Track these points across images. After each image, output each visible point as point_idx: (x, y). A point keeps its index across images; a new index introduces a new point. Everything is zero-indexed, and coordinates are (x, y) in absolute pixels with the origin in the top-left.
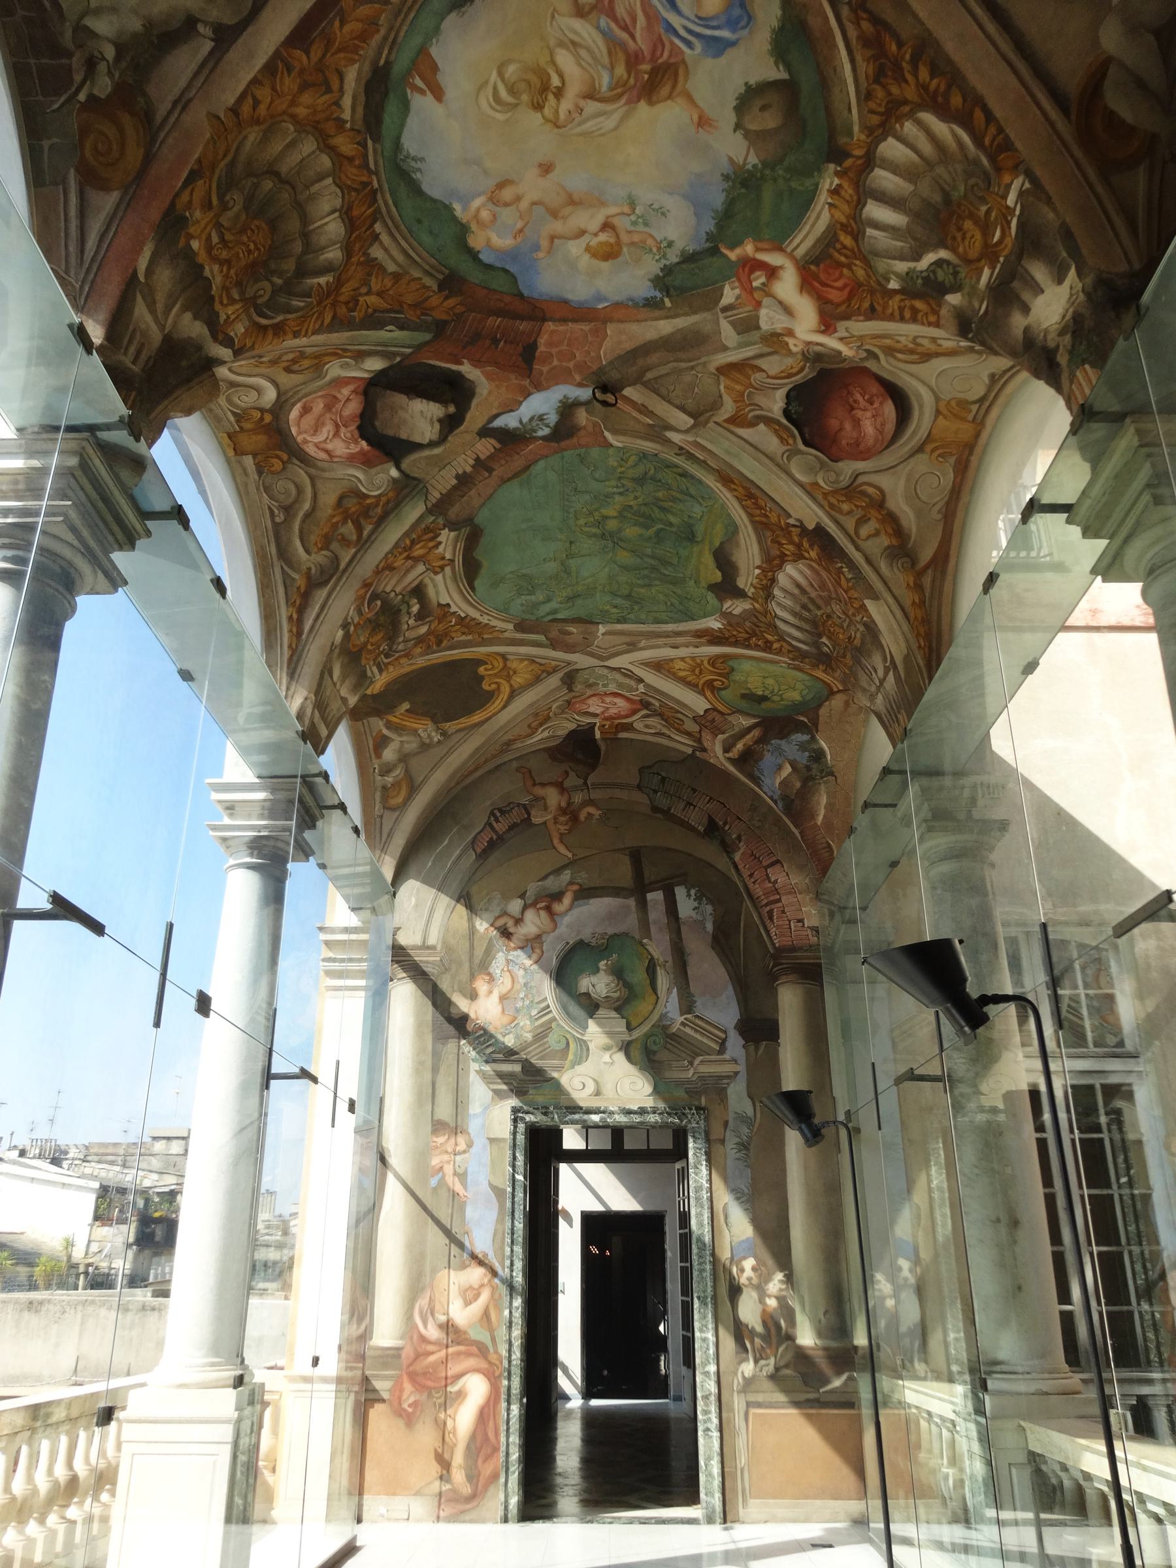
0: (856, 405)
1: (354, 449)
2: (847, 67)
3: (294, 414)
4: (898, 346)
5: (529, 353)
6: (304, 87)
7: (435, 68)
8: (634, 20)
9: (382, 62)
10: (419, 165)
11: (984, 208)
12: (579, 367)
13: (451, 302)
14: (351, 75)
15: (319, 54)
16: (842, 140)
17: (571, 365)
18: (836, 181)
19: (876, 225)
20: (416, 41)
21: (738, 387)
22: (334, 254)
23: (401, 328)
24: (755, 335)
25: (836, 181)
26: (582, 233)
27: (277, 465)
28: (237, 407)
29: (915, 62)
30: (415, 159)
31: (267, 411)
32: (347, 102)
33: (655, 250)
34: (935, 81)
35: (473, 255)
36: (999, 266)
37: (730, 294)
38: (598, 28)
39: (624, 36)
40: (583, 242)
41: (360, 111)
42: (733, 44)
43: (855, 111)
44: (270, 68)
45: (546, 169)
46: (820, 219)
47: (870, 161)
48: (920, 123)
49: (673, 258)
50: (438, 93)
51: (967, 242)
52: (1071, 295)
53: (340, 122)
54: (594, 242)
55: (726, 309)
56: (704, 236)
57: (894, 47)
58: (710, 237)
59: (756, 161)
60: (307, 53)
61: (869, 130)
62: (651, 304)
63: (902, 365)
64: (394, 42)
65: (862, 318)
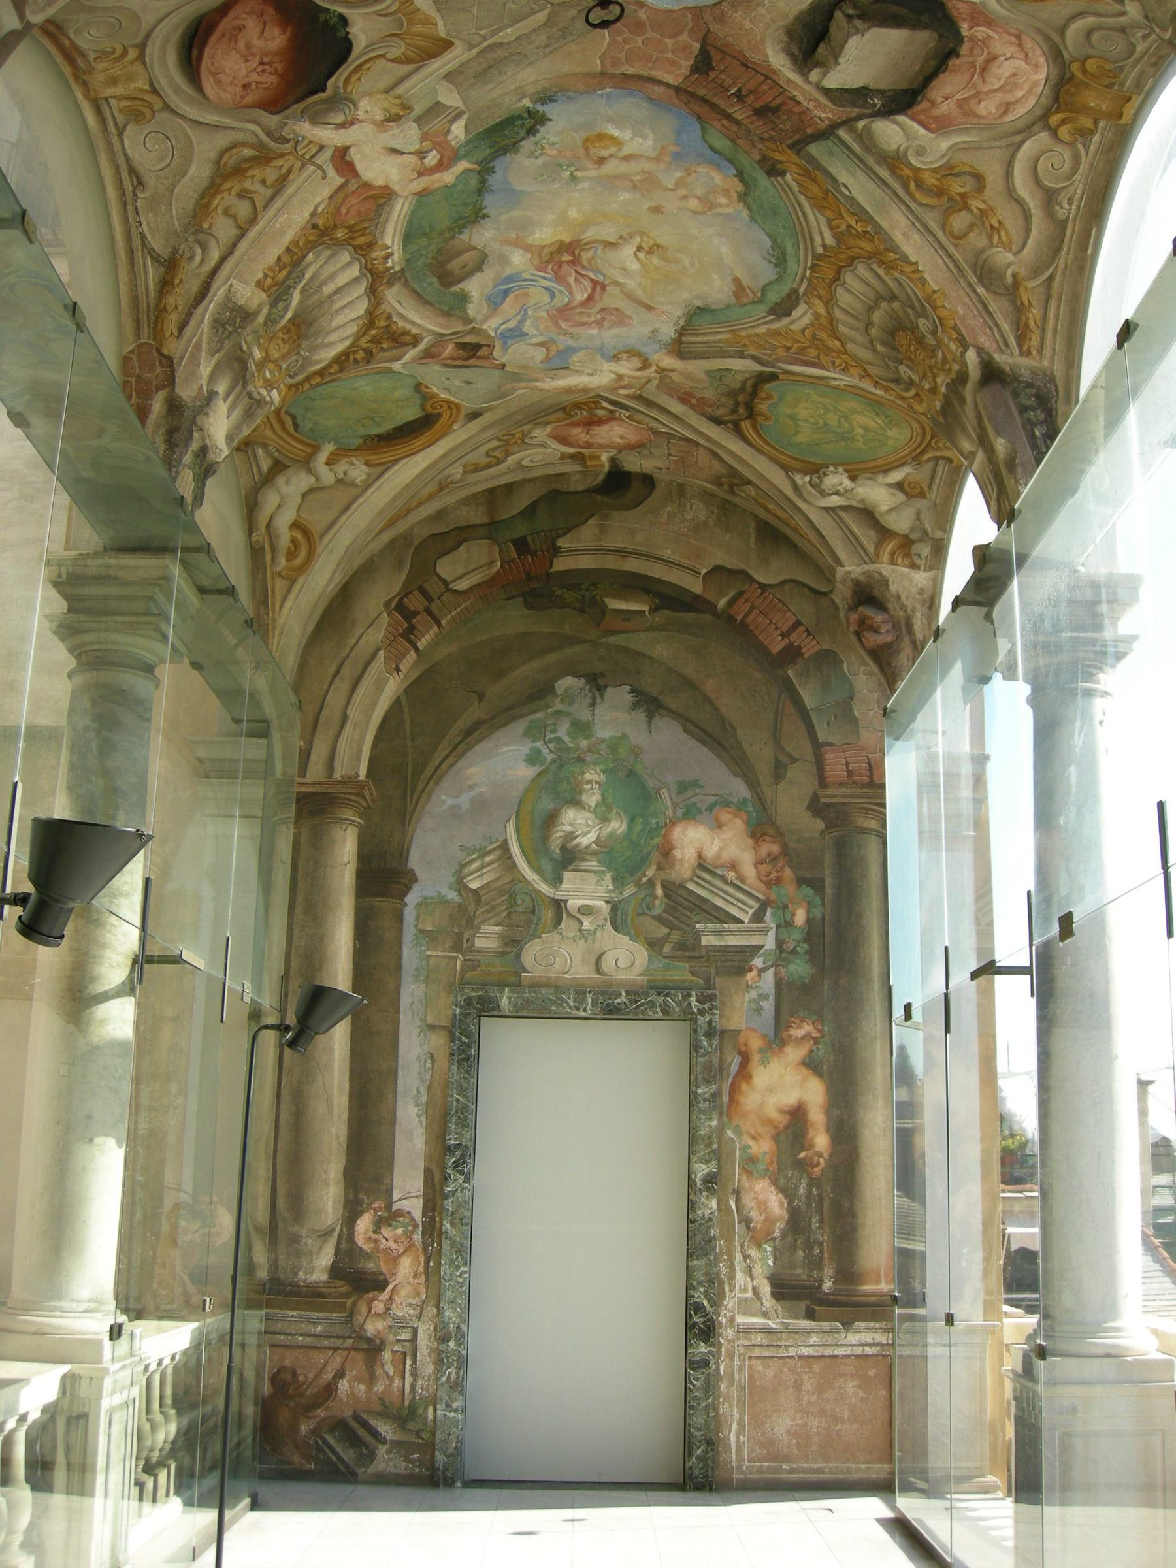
0: (260, 68)
1: (981, 32)
3: (1021, 111)
4: (257, 172)
5: (703, 64)
6: (831, 350)
8: (576, 279)
10: (768, 257)
12: (639, 27)
13: (777, 156)
17: (650, 33)
18: (390, 264)
19: (344, 267)
21: (418, 29)
22: (861, 269)
23: (835, 180)
24: (418, 109)
25: (390, 264)
26: (627, 158)
27: (1091, 65)
28: (1076, 159)
30: (770, 261)
31: (1050, 128)
33: (547, 147)
35: (740, 175)
37: (458, 131)
40: (626, 151)
45: (657, 210)
46: (391, 237)
49: (527, 145)
50: (736, 281)
51: (280, 342)
54: (613, 150)
55: (458, 116)
56: (496, 169)
57: (384, 346)
58: (491, 171)
59: (461, 237)
62: (546, 98)
63: (240, 136)
65: (320, 210)
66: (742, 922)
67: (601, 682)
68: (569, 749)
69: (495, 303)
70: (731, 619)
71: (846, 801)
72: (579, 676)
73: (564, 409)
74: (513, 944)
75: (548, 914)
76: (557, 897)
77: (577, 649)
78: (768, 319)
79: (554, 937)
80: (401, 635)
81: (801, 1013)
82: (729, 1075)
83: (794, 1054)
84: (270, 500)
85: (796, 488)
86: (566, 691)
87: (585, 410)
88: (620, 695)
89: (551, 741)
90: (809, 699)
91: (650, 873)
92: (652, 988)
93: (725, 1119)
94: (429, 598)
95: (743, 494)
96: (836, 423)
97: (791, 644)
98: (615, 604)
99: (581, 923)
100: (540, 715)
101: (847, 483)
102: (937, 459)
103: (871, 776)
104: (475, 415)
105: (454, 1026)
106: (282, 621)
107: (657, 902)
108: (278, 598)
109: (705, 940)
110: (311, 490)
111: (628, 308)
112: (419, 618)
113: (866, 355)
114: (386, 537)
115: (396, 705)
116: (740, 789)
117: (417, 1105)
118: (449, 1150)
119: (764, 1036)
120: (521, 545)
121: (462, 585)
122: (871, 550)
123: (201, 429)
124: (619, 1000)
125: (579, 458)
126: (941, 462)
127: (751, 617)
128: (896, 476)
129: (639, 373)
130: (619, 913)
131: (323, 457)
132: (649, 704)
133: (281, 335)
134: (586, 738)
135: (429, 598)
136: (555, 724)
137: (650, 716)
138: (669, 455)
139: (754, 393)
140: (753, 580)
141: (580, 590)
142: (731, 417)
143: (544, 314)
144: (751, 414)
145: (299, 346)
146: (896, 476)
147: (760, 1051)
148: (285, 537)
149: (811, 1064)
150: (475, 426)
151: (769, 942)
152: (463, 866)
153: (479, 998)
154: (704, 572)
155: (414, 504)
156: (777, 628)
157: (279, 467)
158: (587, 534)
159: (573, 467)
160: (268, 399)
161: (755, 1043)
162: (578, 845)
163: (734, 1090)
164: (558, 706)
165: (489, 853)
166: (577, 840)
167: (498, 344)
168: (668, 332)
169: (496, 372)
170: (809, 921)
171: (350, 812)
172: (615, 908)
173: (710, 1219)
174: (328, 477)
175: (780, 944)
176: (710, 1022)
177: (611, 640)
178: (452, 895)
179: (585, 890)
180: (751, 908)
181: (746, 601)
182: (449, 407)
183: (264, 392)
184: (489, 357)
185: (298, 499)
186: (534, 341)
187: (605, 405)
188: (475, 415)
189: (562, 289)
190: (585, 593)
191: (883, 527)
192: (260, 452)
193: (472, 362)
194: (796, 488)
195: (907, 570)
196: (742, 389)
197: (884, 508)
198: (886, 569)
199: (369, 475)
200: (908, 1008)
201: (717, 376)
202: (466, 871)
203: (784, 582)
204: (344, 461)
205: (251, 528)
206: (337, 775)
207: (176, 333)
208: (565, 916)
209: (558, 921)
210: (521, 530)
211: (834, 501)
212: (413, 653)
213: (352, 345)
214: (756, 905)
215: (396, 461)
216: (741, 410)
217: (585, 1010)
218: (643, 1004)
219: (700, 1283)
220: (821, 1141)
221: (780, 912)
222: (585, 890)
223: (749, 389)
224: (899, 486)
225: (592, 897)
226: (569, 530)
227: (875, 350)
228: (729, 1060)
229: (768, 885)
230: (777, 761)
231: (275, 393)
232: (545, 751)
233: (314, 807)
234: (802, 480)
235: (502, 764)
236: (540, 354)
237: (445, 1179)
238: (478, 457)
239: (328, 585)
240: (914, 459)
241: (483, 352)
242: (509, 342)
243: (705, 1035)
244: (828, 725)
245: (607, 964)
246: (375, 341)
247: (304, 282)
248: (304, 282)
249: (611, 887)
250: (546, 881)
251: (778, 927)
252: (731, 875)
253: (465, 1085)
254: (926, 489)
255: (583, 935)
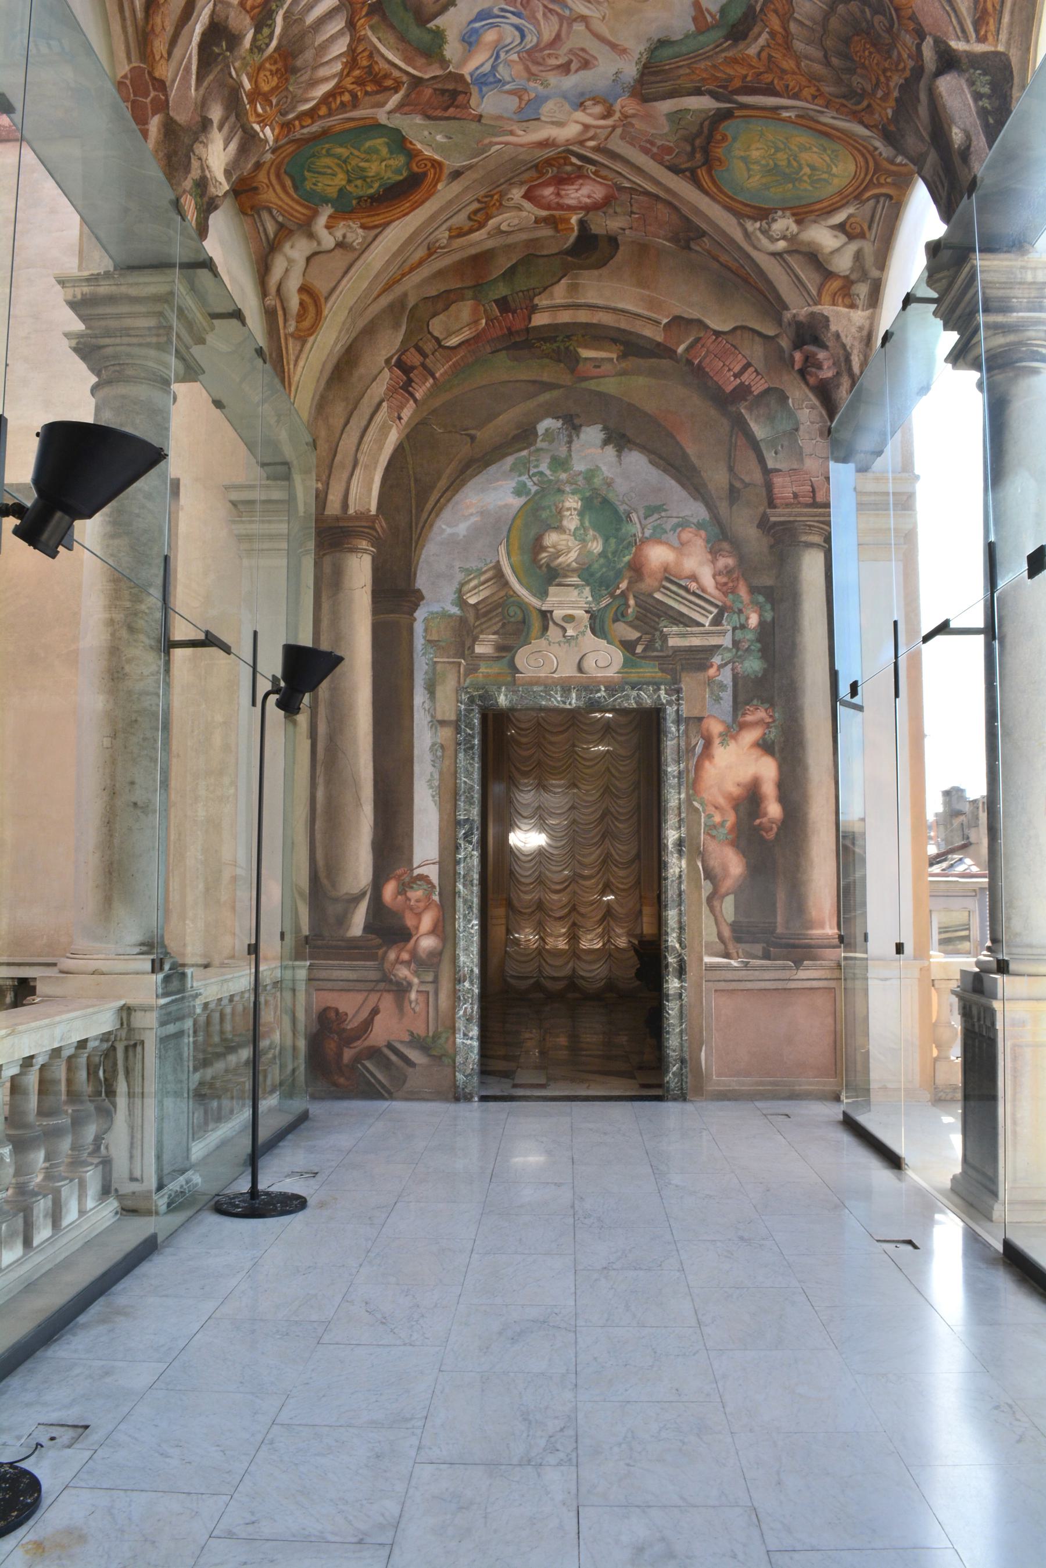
2: (390, 56)
6: (784, 71)
7: (694, 19)
8: (544, 14)
9: (729, 42)
11: (274, 102)
14: (752, 51)
15: (766, 75)
16: (375, 19)
20: (702, 38)
29: (354, 96)
32: (762, 41)
34: (338, 102)
36: (246, 101)
38: (571, 10)
39: (551, 6)
41: (756, 30)
42: (472, 22)
43: (375, 40)
44: (796, 96)
47: (351, 25)
48: (334, 76)
51: (268, 73)
52: (216, 181)
53: (773, 34)
57: (369, 89)
60: (772, 82)
61: (360, 40)
64: (718, 46)
66: (703, 626)
67: (577, 421)
68: (550, 481)
69: (470, 44)
70: (689, 362)
71: (791, 519)
72: (557, 418)
73: (536, 166)
74: (506, 650)
75: (536, 624)
76: (543, 608)
77: (556, 393)
78: (725, 45)
79: (543, 642)
80: (401, 388)
81: (755, 702)
82: (694, 755)
83: (750, 736)
84: (279, 266)
85: (747, 234)
86: (547, 430)
87: (557, 166)
88: (592, 434)
89: (534, 475)
90: (759, 431)
91: (623, 585)
92: (627, 683)
93: (691, 792)
94: (425, 355)
95: (698, 248)
96: (785, 163)
97: (742, 383)
98: (585, 353)
99: (564, 630)
100: (525, 453)
101: (794, 228)
102: (877, 197)
103: (814, 497)
104: (456, 174)
105: (458, 720)
106: (296, 379)
107: (630, 610)
108: (292, 358)
109: (672, 642)
110: (315, 254)
111: (593, 46)
112: (415, 372)
113: (818, 68)
114: (385, 301)
115: (399, 450)
116: (698, 511)
117: (432, 788)
118: (458, 823)
119: (723, 722)
120: (503, 304)
121: (453, 341)
122: (814, 292)
123: (200, 159)
124: (599, 695)
125: (551, 222)
126: (882, 200)
127: (708, 360)
128: (839, 217)
129: (602, 122)
130: (598, 621)
131: (322, 220)
132: (618, 439)
133: (267, 65)
134: (565, 471)
135: (425, 355)
136: (537, 460)
137: (620, 450)
138: (632, 212)
139: (710, 138)
140: (706, 327)
141: (556, 342)
142: (688, 165)
143: (515, 57)
144: (709, 162)
145: (287, 80)
146: (839, 217)
147: (720, 735)
148: (294, 302)
149: (765, 746)
150: (456, 187)
151: (727, 641)
152: (462, 585)
153: (480, 696)
154: (665, 321)
155: (407, 269)
156: (729, 370)
157: (284, 232)
158: (559, 293)
159: (546, 232)
160: (261, 135)
161: (716, 728)
162: (560, 564)
163: (698, 767)
164: (540, 444)
165: (485, 572)
166: (560, 560)
167: (474, 90)
168: (630, 70)
169: (474, 125)
170: (762, 623)
171: (364, 543)
172: (593, 616)
173: (680, 876)
174: (328, 241)
175: (736, 643)
176: (678, 710)
177: (584, 385)
178: (455, 610)
179: (570, 601)
180: (711, 613)
181: (703, 346)
182: (433, 166)
183: (257, 127)
184: (467, 106)
185: (302, 263)
186: (507, 87)
187: (574, 160)
188: (456, 174)
189: (531, 27)
190: (559, 344)
191: (826, 270)
192: (265, 216)
193: (451, 111)
194: (747, 234)
195: (847, 310)
196: (700, 133)
197: (828, 250)
198: (826, 309)
199: (364, 238)
200: (854, 688)
201: (676, 117)
202: (465, 589)
203: (735, 329)
204: (342, 224)
205: (264, 293)
206: (351, 511)
207: (165, 55)
208: (551, 623)
209: (545, 629)
210: (502, 290)
211: (782, 245)
212: (412, 402)
213: (337, 86)
214: (715, 611)
215: (386, 225)
216: (698, 156)
217: (570, 704)
218: (620, 697)
219: (673, 930)
220: (774, 810)
221: (735, 617)
222: (570, 601)
223: (706, 130)
224: (841, 227)
225: (574, 608)
226: (545, 289)
227: (828, 63)
228: (693, 743)
229: (725, 594)
230: (731, 486)
231: (268, 129)
232: (529, 484)
233: (333, 536)
234: (752, 226)
235: (493, 496)
236: (511, 103)
237: (457, 848)
238: (461, 219)
239: (336, 344)
240: (856, 198)
241: (461, 98)
242: (484, 89)
243: (673, 722)
244: (776, 453)
245: (589, 664)
246: (360, 82)
247: (286, 6)
248: (286, 6)
249: (590, 599)
250: (534, 595)
251: (734, 629)
252: (693, 586)
253: (470, 769)
254: (866, 227)
255: (569, 640)
